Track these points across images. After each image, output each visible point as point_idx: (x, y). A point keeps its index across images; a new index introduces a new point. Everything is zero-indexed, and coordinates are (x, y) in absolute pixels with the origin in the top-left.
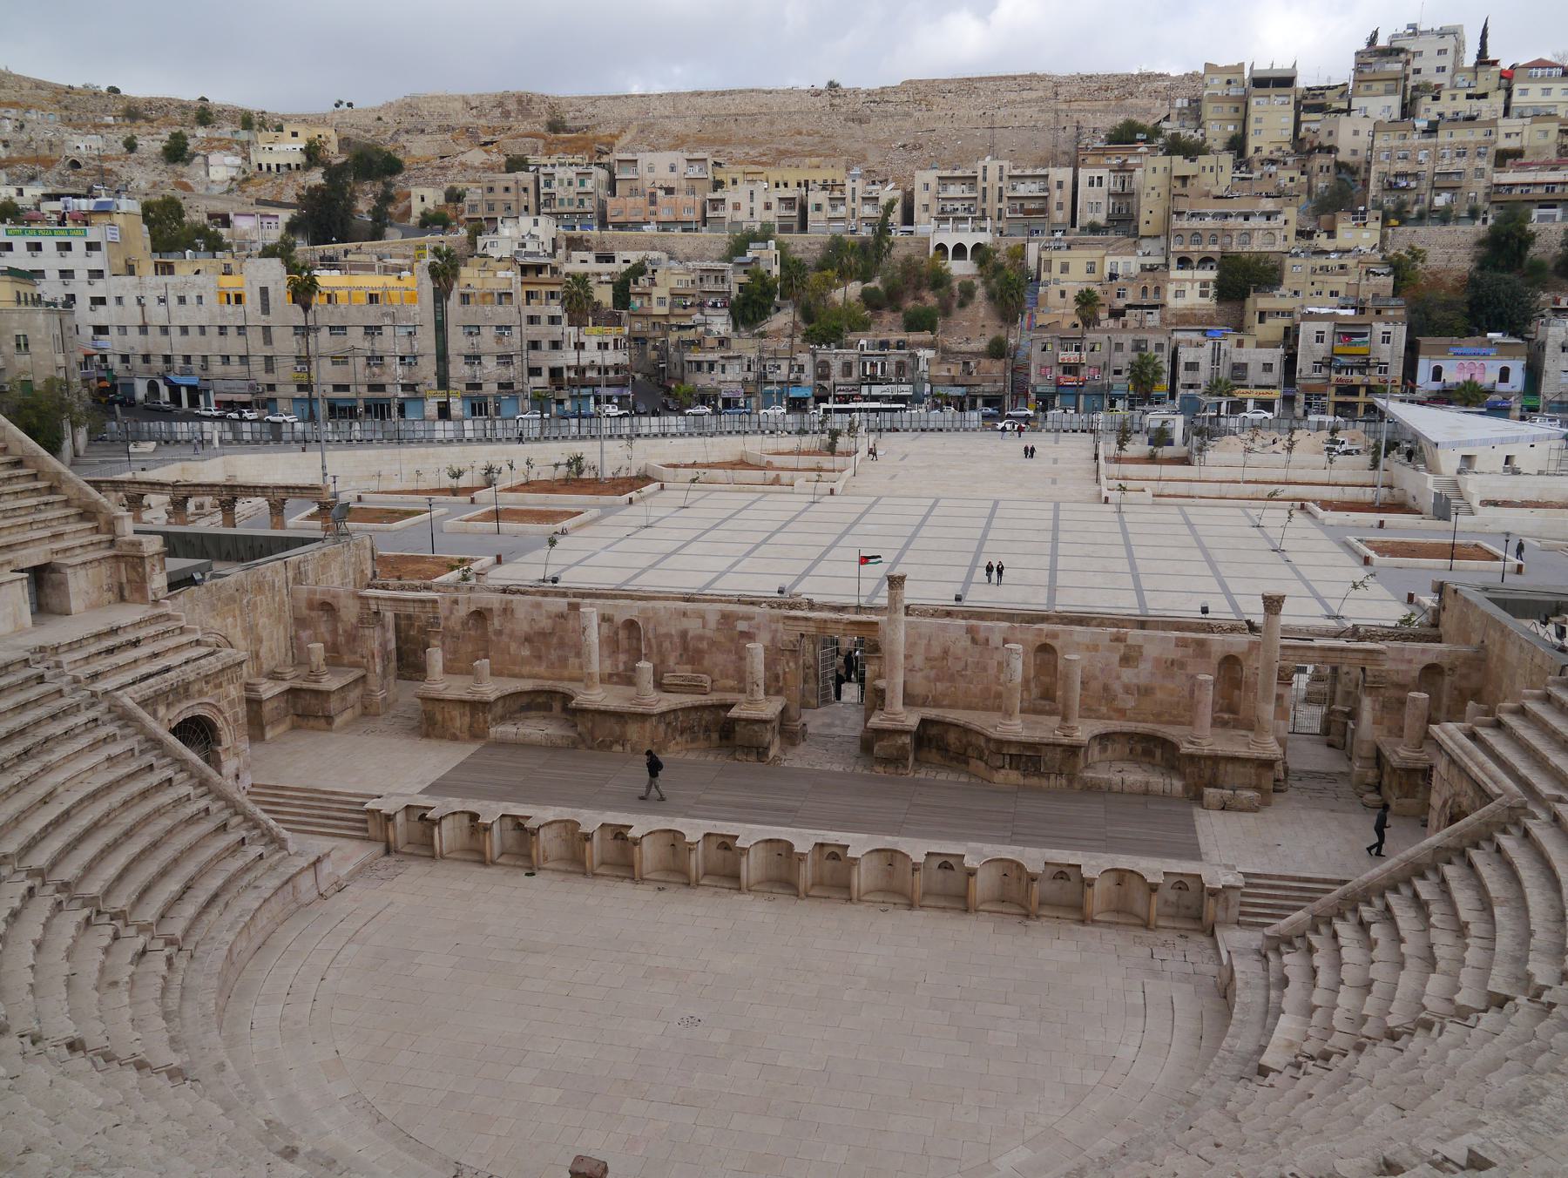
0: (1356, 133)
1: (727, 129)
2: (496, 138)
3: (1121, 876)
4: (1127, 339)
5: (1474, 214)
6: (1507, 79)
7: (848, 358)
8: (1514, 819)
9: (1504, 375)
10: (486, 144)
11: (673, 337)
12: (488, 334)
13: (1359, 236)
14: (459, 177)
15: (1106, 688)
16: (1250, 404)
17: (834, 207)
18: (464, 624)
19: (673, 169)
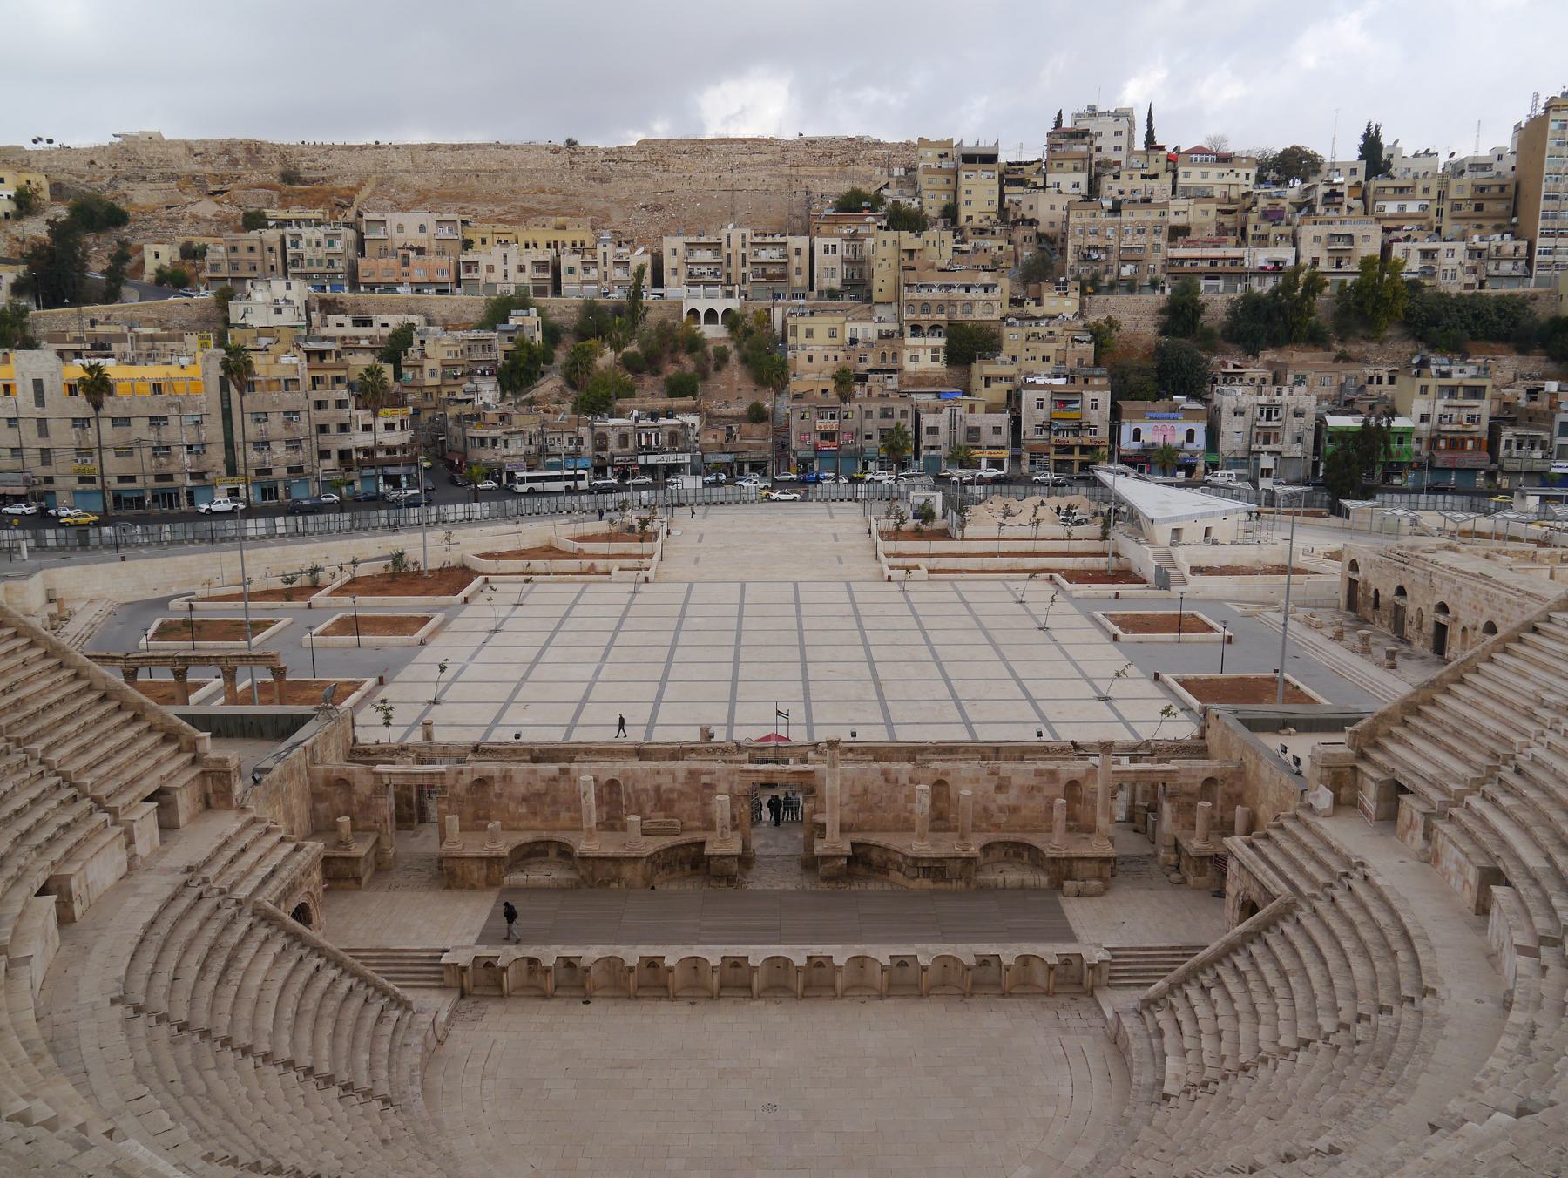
0: (1053, 207)
1: (469, 188)
2: (225, 187)
3: (1025, 960)
4: (876, 407)
5: (1154, 285)
6: (1174, 160)
7: (625, 430)
8: (1288, 910)
9: (1190, 435)
10: (214, 193)
11: (453, 411)
12: (276, 421)
13: (1061, 304)
14: (192, 230)
15: (986, 809)
16: (984, 463)
17: (586, 271)
18: (468, 790)
19: (422, 229)
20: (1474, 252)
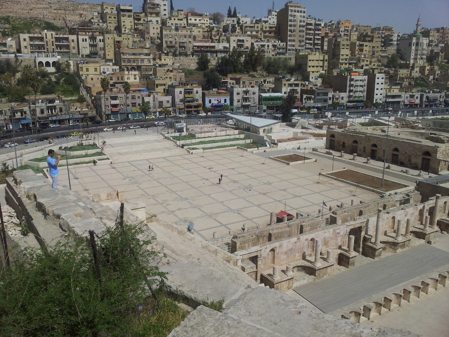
0: (154, 28)
9: (225, 101)
20: (274, 46)
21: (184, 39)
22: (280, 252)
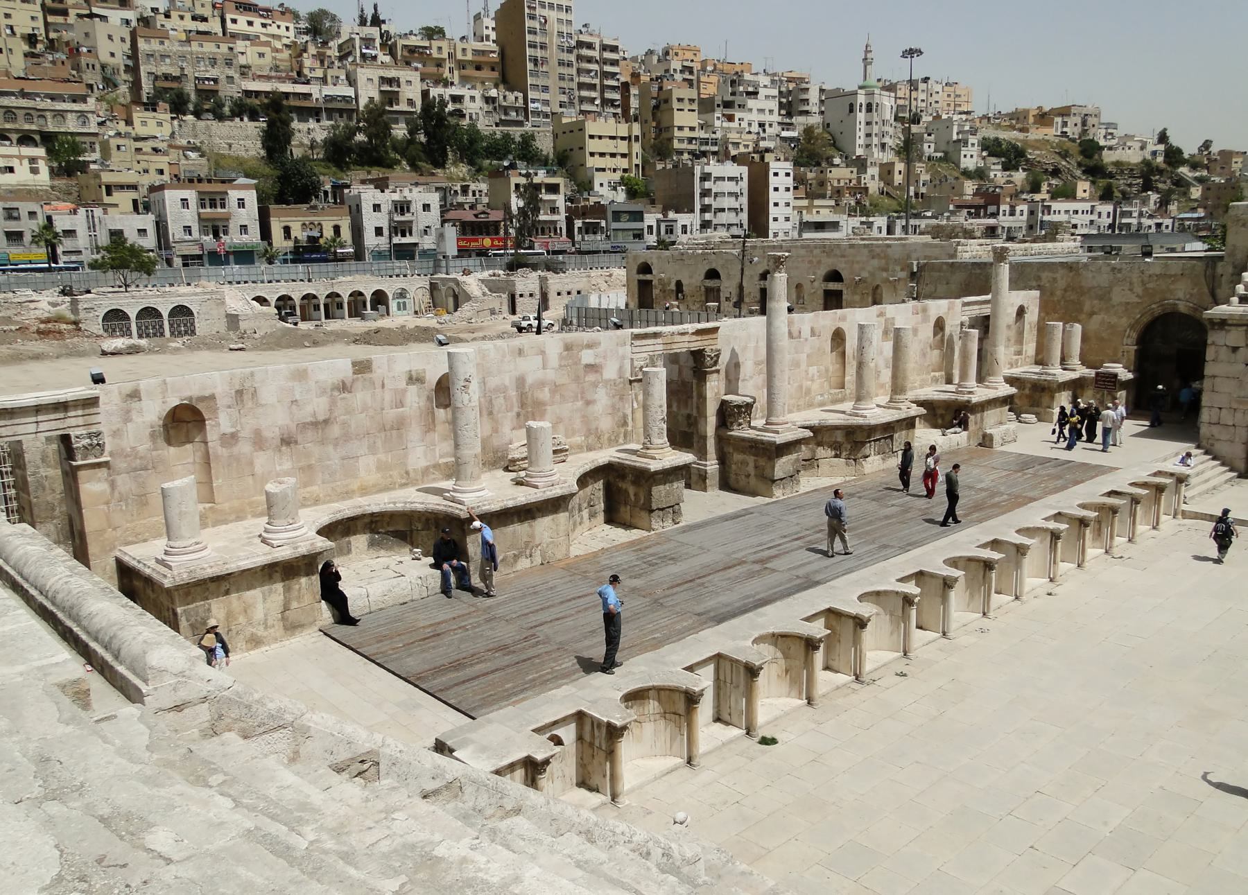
21: (209, 68)
22: (246, 433)
